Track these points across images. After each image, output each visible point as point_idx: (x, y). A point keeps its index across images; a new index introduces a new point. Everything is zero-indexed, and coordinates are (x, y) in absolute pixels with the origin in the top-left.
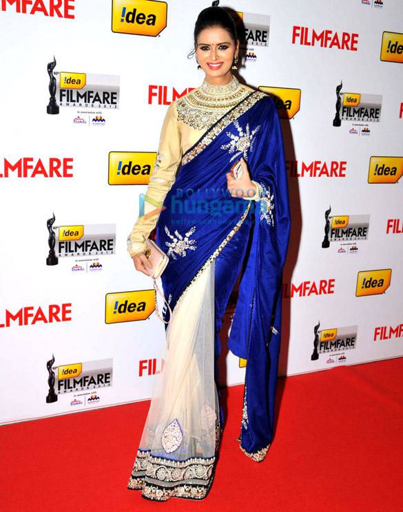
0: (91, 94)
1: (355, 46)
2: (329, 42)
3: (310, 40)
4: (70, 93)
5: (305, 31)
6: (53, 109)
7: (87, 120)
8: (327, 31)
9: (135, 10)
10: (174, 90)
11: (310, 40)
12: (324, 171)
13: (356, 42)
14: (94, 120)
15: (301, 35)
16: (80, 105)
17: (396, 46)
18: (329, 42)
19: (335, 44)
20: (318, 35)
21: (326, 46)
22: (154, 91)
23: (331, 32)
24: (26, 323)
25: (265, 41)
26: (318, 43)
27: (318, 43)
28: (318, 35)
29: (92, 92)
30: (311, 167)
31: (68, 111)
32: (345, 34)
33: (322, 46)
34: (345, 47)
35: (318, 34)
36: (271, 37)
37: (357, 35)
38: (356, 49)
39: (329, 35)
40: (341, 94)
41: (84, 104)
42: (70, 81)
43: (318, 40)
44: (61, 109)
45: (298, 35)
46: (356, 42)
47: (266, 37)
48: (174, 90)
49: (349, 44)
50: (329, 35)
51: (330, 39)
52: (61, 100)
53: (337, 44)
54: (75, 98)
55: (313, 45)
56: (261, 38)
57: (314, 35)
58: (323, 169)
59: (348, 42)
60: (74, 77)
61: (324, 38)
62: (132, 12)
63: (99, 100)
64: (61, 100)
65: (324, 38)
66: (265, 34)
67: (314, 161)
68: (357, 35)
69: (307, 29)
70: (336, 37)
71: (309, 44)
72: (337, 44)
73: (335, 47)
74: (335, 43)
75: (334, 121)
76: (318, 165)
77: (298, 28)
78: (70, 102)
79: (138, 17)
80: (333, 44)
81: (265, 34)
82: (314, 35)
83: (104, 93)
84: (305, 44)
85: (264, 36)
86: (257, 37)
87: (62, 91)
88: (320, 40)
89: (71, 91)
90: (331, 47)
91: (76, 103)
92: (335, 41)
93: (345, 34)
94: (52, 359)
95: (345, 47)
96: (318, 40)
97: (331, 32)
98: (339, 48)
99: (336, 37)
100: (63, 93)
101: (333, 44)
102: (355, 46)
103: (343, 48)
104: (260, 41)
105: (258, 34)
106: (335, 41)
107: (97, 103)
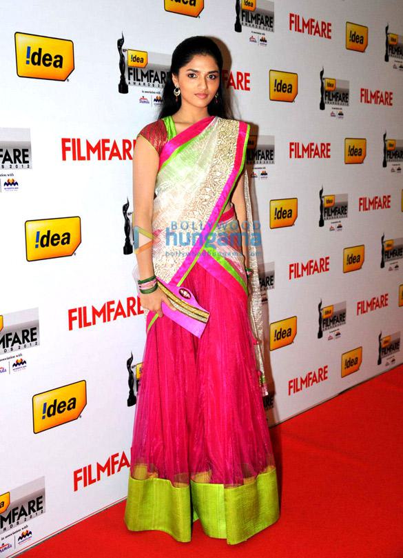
0: (152, 74)
2: (108, 154)
3: (84, 153)
4: (136, 70)
6: (123, 88)
7: (149, 100)
8: (103, 140)
9: (40, 50)
10: (88, 142)
11: (84, 153)
12: (120, 312)
14: (5, 184)
15: (70, 148)
16: (144, 84)
17: (48, 236)
18: (108, 154)
19: (115, 155)
20: (94, 146)
21: (104, 159)
22: (69, 145)
23: (108, 141)
24: (109, 320)
25: (28, 162)
26: (94, 156)
27: (94, 156)
28: (94, 146)
29: (153, 71)
30: (103, 310)
31: (135, 90)
32: (125, 141)
33: (99, 159)
34: (127, 157)
36: (34, 156)
39: (107, 145)
40: (129, 214)
41: (147, 83)
42: (135, 59)
43: (94, 152)
44: (130, 88)
45: (69, 149)
47: (27, 156)
48: (88, 142)
50: (107, 145)
51: (108, 149)
52: (129, 79)
53: (118, 154)
54: (140, 77)
55: (89, 159)
56: (21, 158)
58: (118, 309)
60: (139, 55)
62: (38, 52)
63: (158, 80)
64: (129, 79)
66: (26, 153)
67: (106, 301)
69: (79, 140)
70: (115, 146)
71: (83, 158)
72: (118, 154)
73: (115, 158)
75: (124, 248)
76: (112, 307)
77: (68, 140)
78: (136, 81)
79: (44, 59)
80: (112, 155)
81: (26, 153)
83: (162, 73)
84: (79, 159)
85: (25, 156)
86: (16, 157)
87: (130, 69)
88: (97, 152)
89: (137, 70)
90: (110, 159)
91: (141, 82)
92: (115, 151)
93: (125, 141)
94: (130, 357)
95: (127, 157)
96: (94, 152)
97: (108, 141)
98: (120, 159)
99: (115, 146)
100: (131, 71)
101: (112, 155)
103: (125, 158)
104: (20, 162)
105: (17, 154)
106: (115, 151)
107: (157, 83)
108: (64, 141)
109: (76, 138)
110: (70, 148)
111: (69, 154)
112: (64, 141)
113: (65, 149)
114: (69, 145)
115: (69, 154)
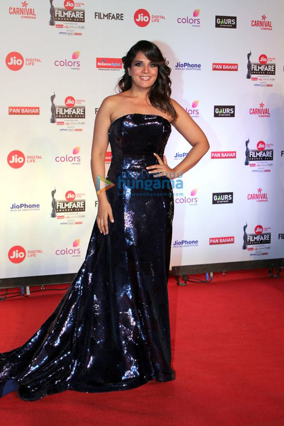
1: (122, 18)
2: (111, 18)
3: (102, 17)
5: (100, 14)
11: (102, 17)
13: (123, 17)
15: (98, 15)
18: (111, 18)
20: (106, 15)
26: (106, 18)
32: (117, 14)
35: (106, 15)
37: (123, 14)
38: (123, 20)
46: (123, 17)
49: (120, 18)
53: (114, 18)
57: (104, 15)
59: (119, 17)
61: (108, 16)
65: (108, 16)
68: (123, 14)
70: (113, 15)
72: (114, 18)
74: (113, 17)
80: (112, 18)
82: (104, 15)
99: (113, 15)
101: (112, 18)
102: (122, 18)
108: (96, 13)
109: (100, 12)
110: (98, 15)
111: (97, 17)
112: (96, 13)
113: (96, 15)
114: (97, 14)
115: (97, 17)
